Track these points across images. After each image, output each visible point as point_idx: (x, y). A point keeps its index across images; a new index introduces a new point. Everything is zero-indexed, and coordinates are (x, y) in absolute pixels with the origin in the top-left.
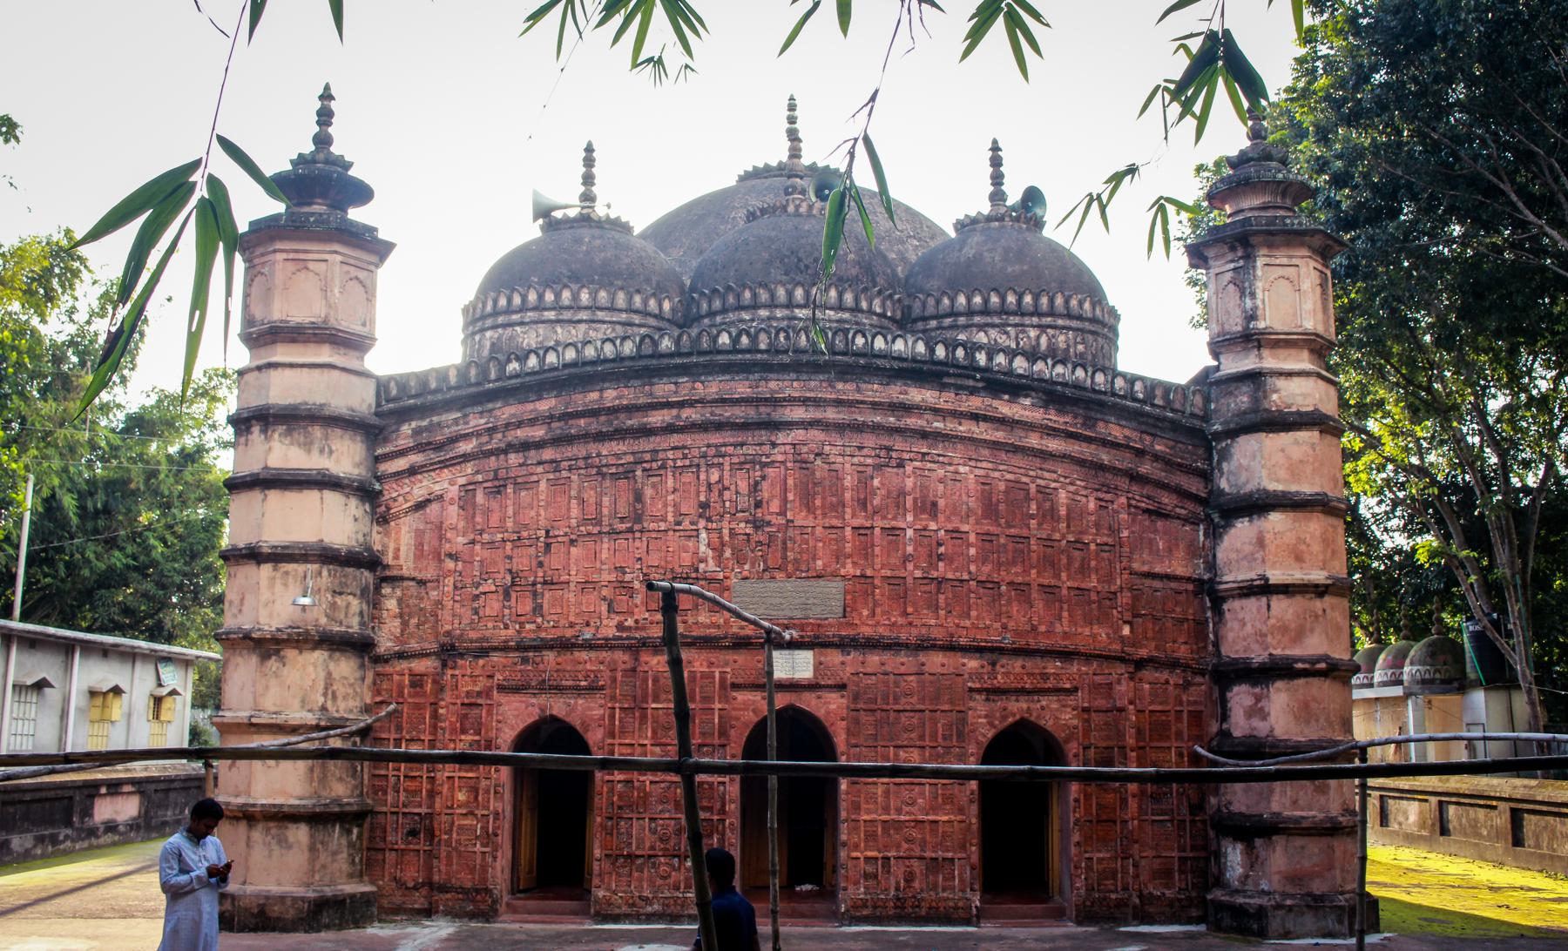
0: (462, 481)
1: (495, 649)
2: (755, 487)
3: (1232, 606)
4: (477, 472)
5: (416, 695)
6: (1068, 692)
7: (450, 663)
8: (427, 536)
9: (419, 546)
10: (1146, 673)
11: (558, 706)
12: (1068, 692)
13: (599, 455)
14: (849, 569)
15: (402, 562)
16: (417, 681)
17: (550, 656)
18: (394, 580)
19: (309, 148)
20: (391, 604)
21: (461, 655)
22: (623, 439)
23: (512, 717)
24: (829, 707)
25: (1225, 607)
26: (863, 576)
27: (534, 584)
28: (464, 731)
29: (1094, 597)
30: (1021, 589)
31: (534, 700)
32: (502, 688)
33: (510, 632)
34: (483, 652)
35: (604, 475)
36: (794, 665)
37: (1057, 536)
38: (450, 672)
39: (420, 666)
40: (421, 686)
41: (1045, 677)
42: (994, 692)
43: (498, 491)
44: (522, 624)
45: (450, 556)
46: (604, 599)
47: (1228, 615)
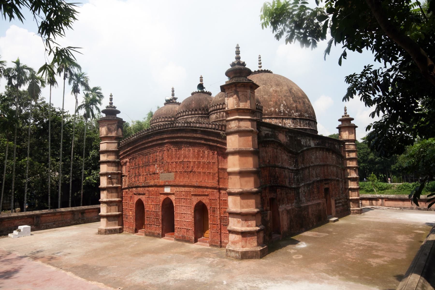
2: (162, 156)
6: (208, 195)
10: (221, 191)
12: (208, 195)
14: (174, 170)
17: (134, 189)
18: (124, 176)
19: (108, 105)
20: (123, 180)
23: (136, 198)
24: (173, 198)
29: (212, 174)
30: (200, 173)
32: (135, 194)
36: (167, 190)
37: (205, 161)
41: (203, 192)
42: (195, 195)
43: (133, 159)
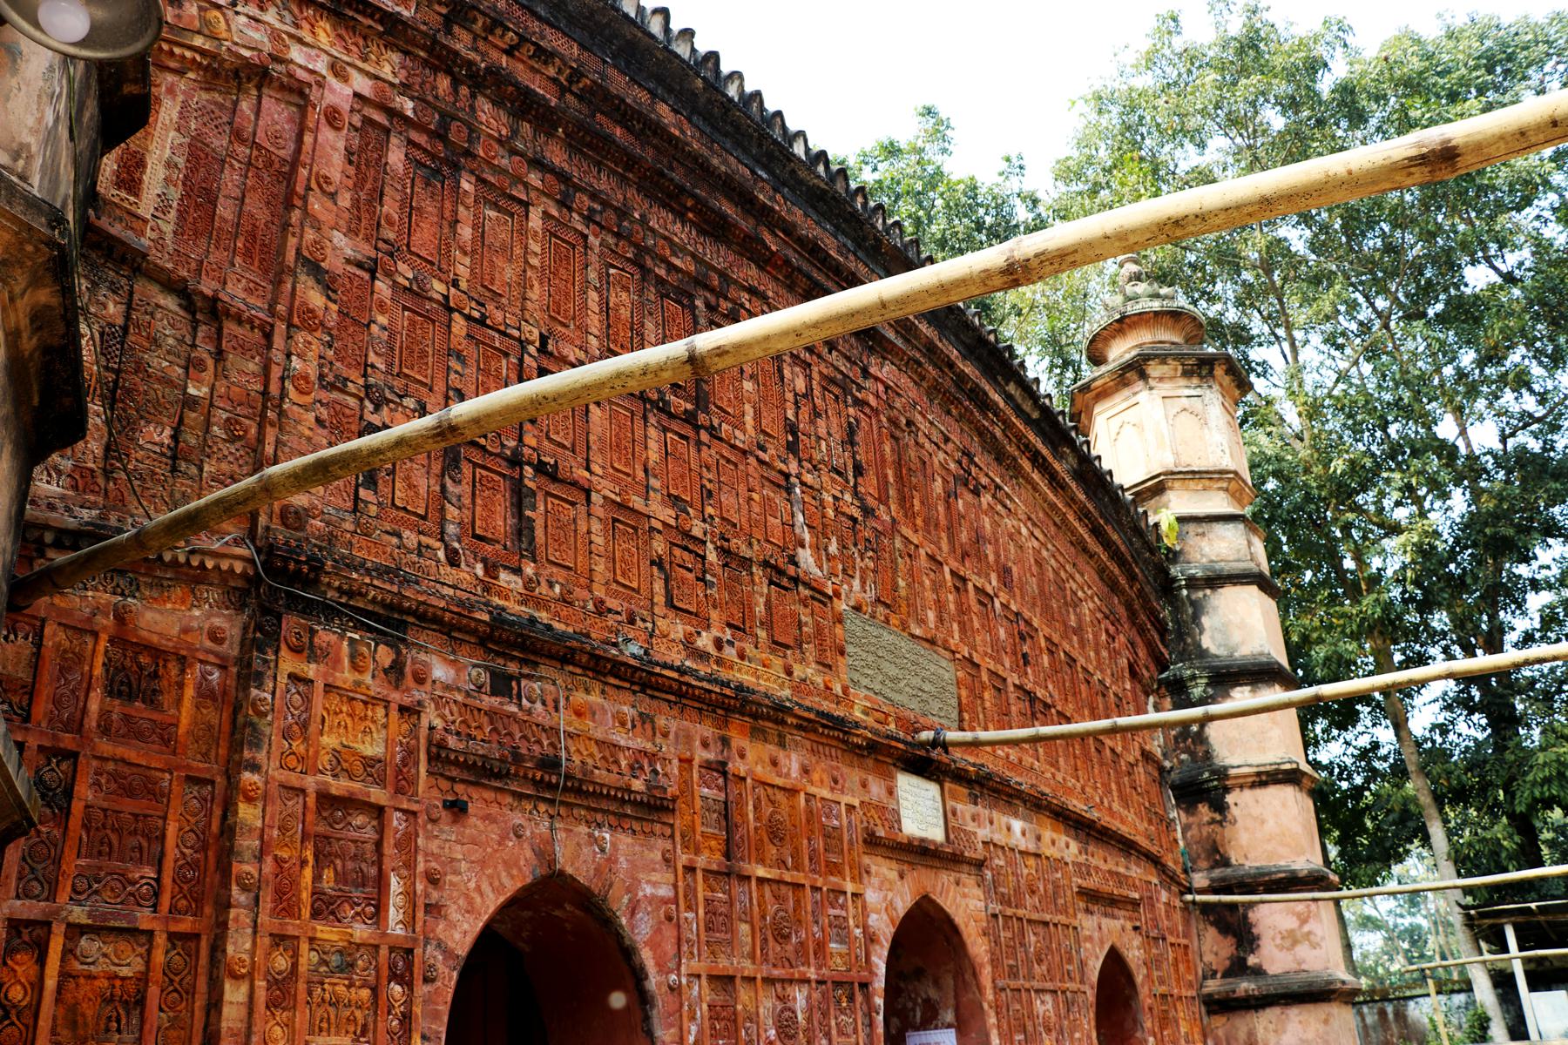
0: (362, 84)
1: (427, 618)
3: (1241, 802)
4: (405, 89)
5: (132, 731)
7: (291, 624)
8: (230, 180)
9: (198, 195)
11: (582, 849)
13: (644, 220)
15: (146, 208)
16: (140, 672)
21: (329, 612)
22: (680, 215)
25: (1230, 799)
26: (970, 661)
27: (516, 461)
28: (325, 908)
31: (517, 819)
33: (463, 575)
34: (394, 621)
35: (645, 271)
38: (288, 663)
39: (162, 618)
40: (151, 699)
44: (492, 570)
45: (315, 269)
46: (658, 563)
47: (1234, 811)
